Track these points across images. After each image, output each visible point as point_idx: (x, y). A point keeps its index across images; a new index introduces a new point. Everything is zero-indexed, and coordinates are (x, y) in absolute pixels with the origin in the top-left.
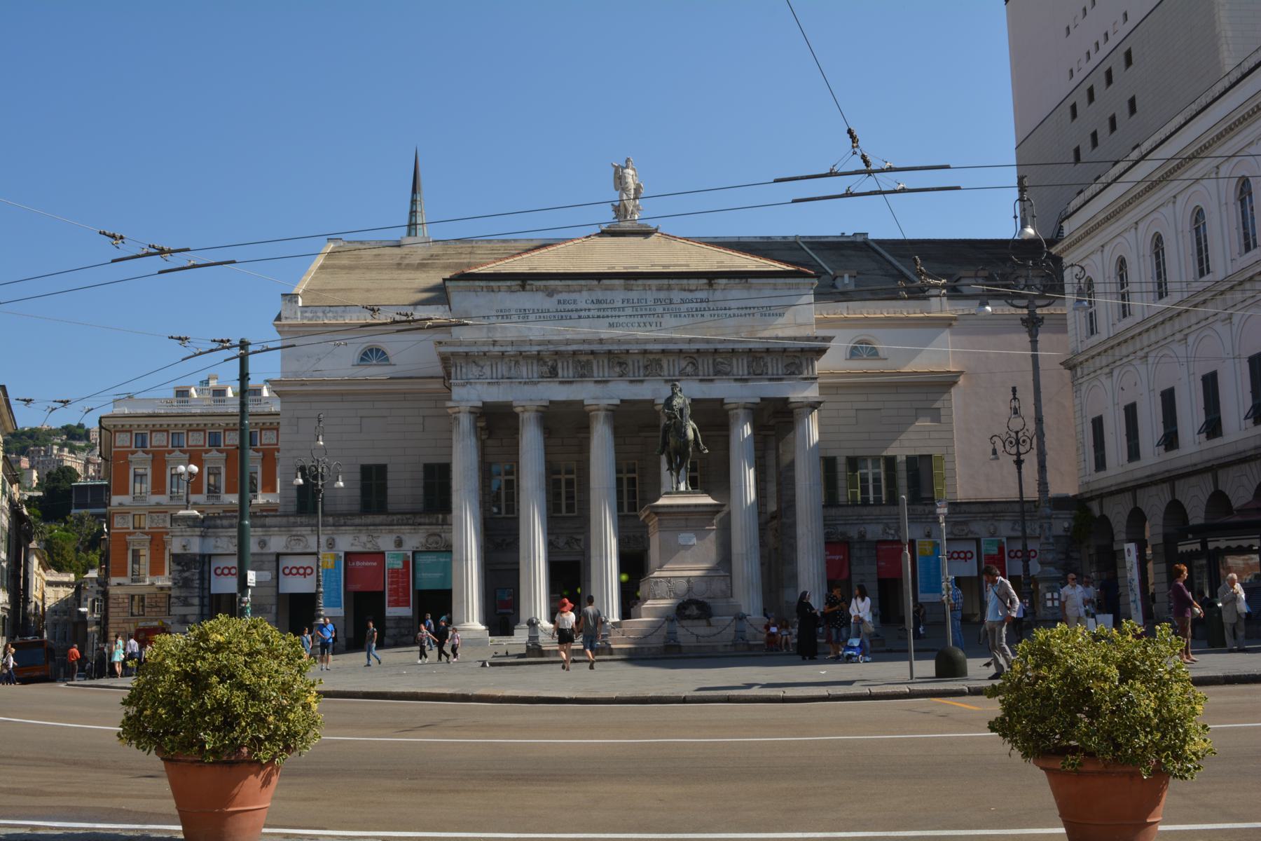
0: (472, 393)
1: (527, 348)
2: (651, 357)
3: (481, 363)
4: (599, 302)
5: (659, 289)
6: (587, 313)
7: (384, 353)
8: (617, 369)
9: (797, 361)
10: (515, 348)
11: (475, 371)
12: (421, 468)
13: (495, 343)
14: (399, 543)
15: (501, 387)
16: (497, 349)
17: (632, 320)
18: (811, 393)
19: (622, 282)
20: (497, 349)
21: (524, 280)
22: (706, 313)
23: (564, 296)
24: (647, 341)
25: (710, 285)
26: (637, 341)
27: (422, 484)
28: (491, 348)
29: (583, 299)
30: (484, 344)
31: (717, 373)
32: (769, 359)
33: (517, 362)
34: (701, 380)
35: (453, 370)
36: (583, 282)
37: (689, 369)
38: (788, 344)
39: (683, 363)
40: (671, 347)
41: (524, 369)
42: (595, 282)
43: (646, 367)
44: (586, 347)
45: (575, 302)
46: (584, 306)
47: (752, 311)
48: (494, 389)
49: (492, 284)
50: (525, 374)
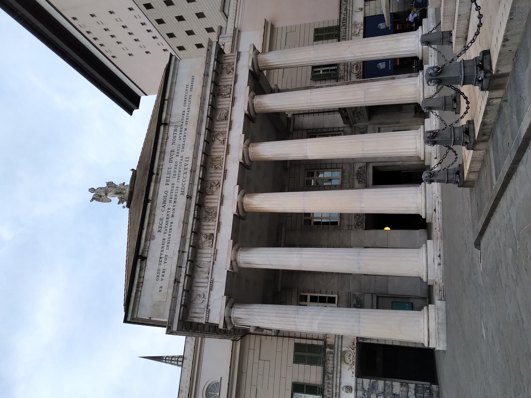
0: (214, 305)
1: (186, 255)
3: (195, 295)
4: (164, 202)
5: (162, 158)
6: (171, 211)
7: (213, 386)
8: (214, 188)
10: (184, 265)
12: (296, 366)
13: (177, 281)
14: (349, 389)
15: (214, 280)
16: (182, 280)
17: (181, 178)
19: (153, 184)
22: (184, 127)
23: (156, 227)
24: (194, 164)
25: (166, 124)
26: (193, 171)
27: (308, 366)
29: (160, 214)
30: (175, 290)
31: (226, 118)
34: (230, 129)
35: (196, 320)
38: (211, 69)
39: (217, 142)
40: (201, 148)
41: (205, 260)
42: (149, 204)
45: (161, 219)
46: (165, 213)
47: (188, 97)
48: (216, 286)
49: (136, 283)
50: (209, 260)
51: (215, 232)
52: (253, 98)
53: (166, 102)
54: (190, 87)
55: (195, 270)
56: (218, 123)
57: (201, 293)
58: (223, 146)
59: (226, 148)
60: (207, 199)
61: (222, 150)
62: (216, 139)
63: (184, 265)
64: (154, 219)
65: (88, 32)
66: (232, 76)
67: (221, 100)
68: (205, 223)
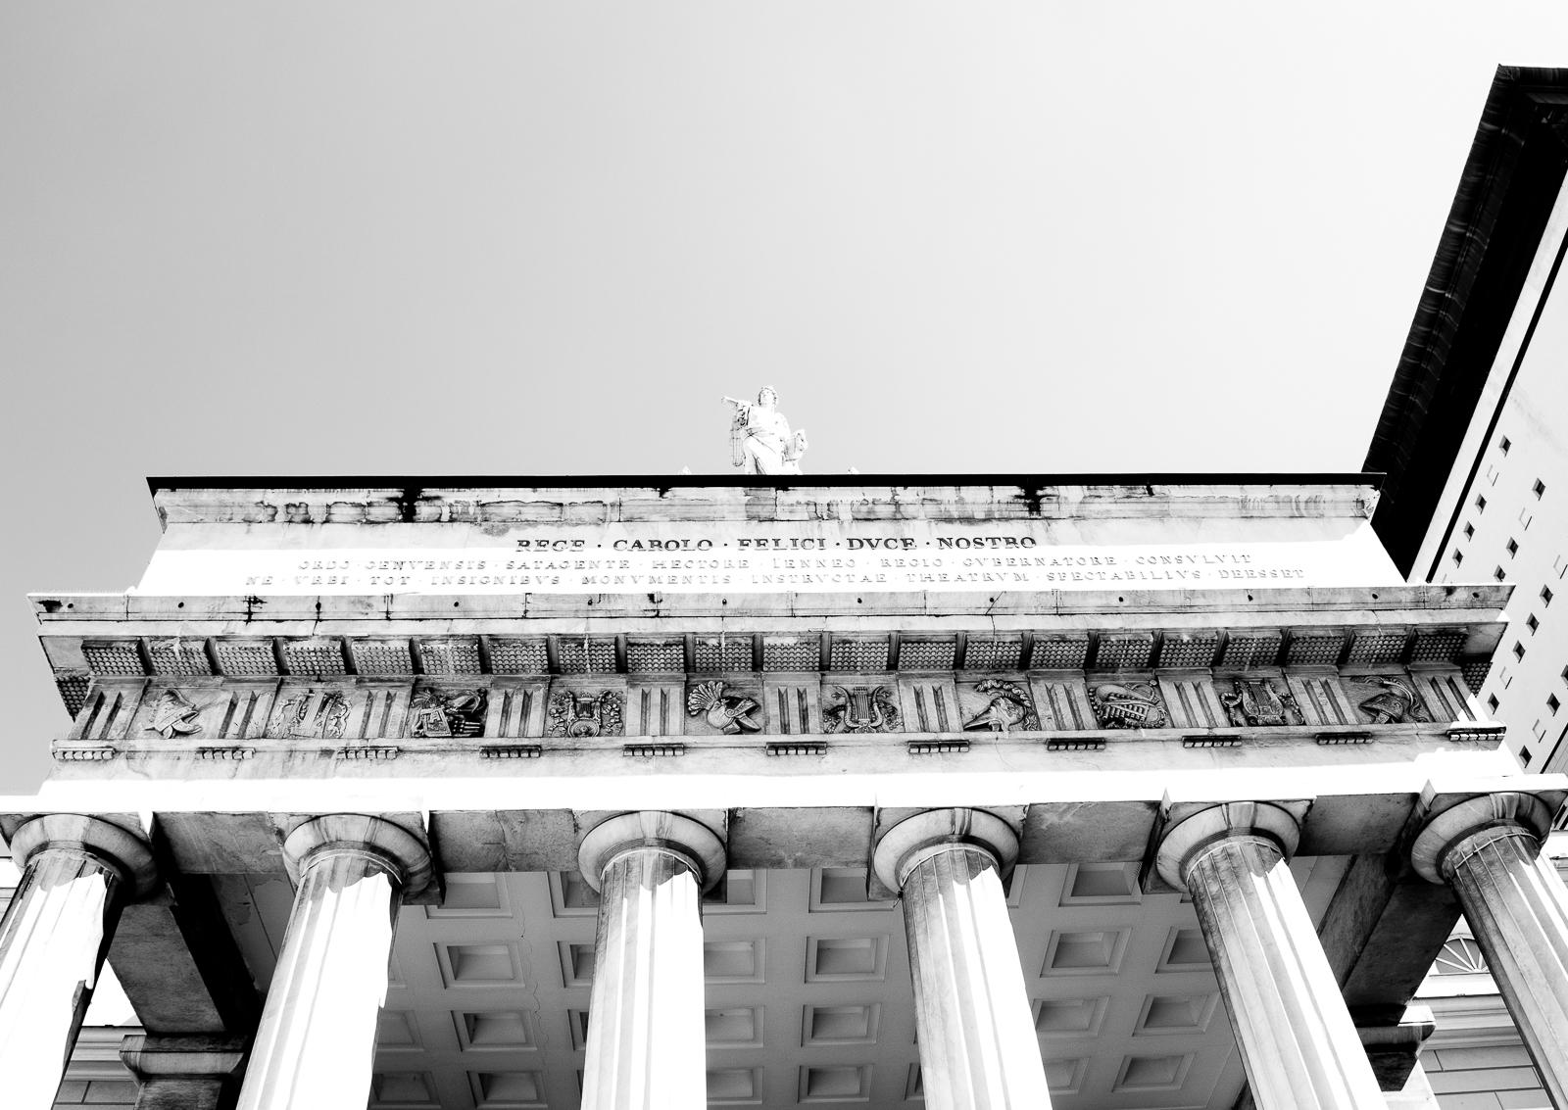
2: (850, 682)
3: (197, 700)
8: (720, 716)
9: (1399, 689)
11: (166, 713)
16: (257, 629)
18: (1497, 773)
20: (257, 629)
21: (410, 494)
25: (1034, 506)
28: (239, 628)
32: (1296, 683)
33: (333, 700)
36: (609, 495)
37: (1002, 713)
39: (975, 703)
42: (650, 494)
43: (832, 713)
44: (601, 628)
47: (1186, 564)
51: (491, 738)
52: (1255, 831)
53: (1141, 490)
54: (1242, 566)
55: (318, 686)
56: (1079, 692)
57: (199, 720)
58: (955, 722)
59: (945, 736)
60: (664, 696)
61: (933, 721)
62: (993, 695)
63: (322, 629)
64: (580, 523)
65: (1482, 503)
66: (1354, 720)
67: (1208, 689)
68: (538, 696)
